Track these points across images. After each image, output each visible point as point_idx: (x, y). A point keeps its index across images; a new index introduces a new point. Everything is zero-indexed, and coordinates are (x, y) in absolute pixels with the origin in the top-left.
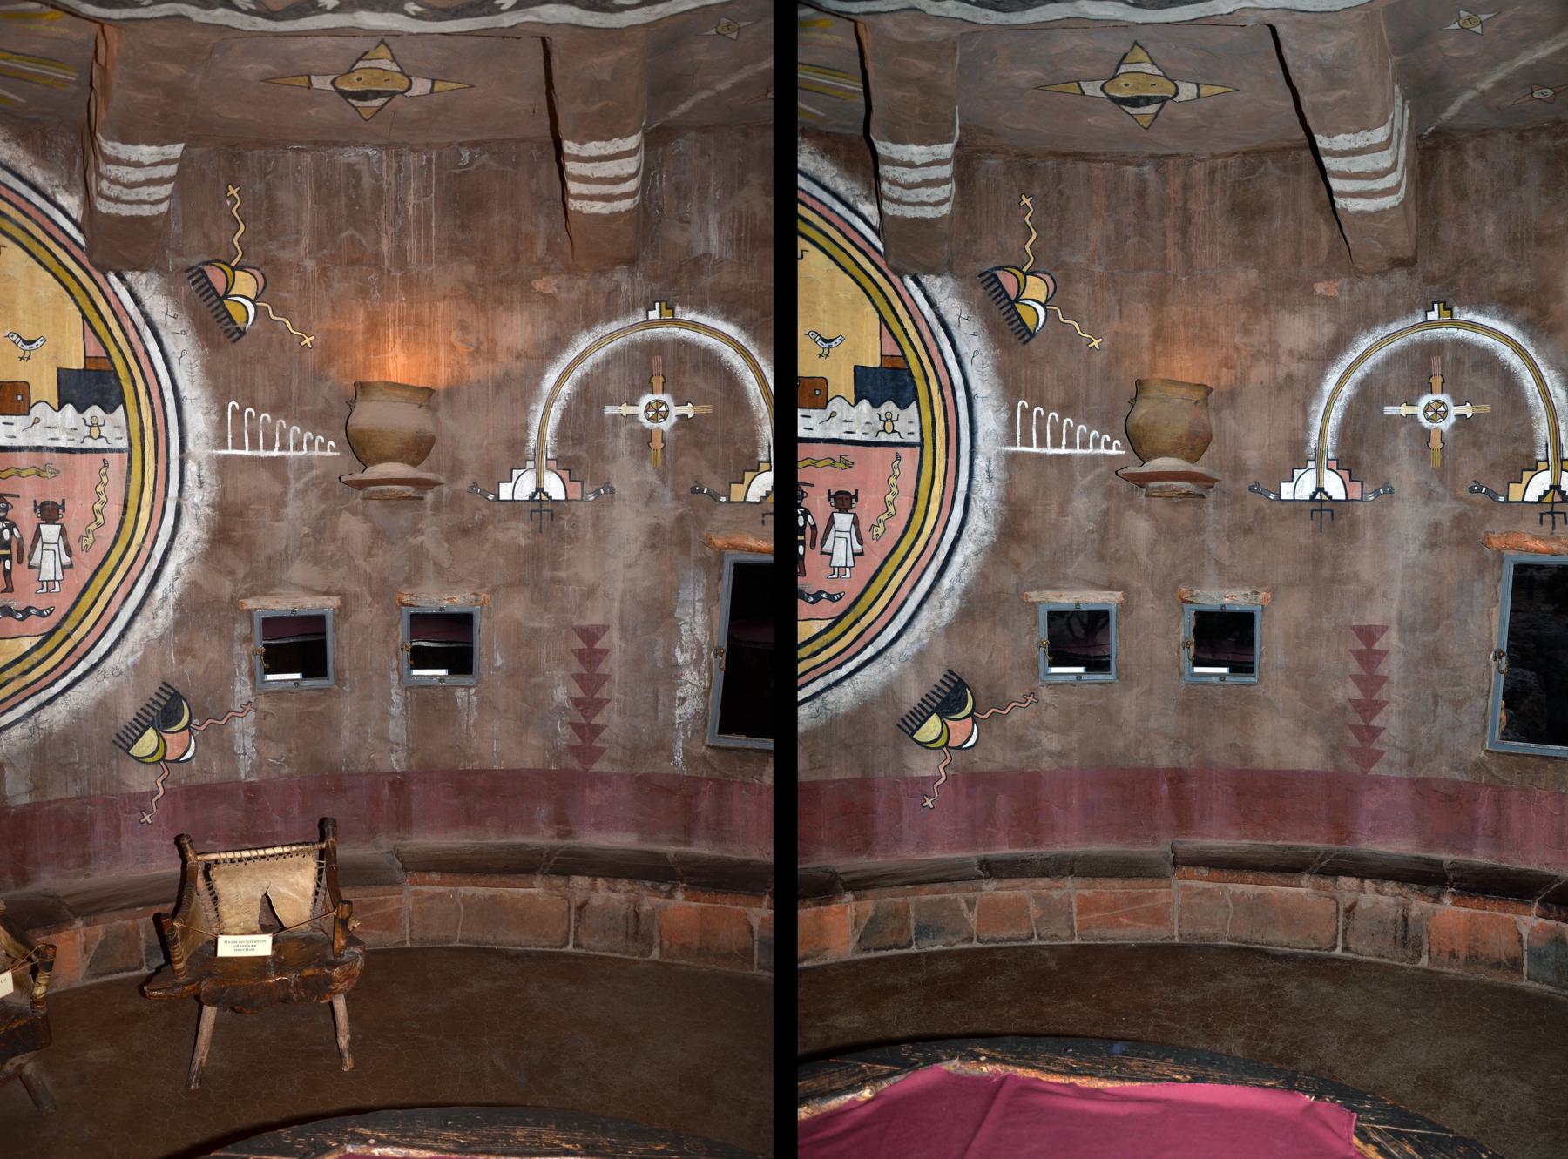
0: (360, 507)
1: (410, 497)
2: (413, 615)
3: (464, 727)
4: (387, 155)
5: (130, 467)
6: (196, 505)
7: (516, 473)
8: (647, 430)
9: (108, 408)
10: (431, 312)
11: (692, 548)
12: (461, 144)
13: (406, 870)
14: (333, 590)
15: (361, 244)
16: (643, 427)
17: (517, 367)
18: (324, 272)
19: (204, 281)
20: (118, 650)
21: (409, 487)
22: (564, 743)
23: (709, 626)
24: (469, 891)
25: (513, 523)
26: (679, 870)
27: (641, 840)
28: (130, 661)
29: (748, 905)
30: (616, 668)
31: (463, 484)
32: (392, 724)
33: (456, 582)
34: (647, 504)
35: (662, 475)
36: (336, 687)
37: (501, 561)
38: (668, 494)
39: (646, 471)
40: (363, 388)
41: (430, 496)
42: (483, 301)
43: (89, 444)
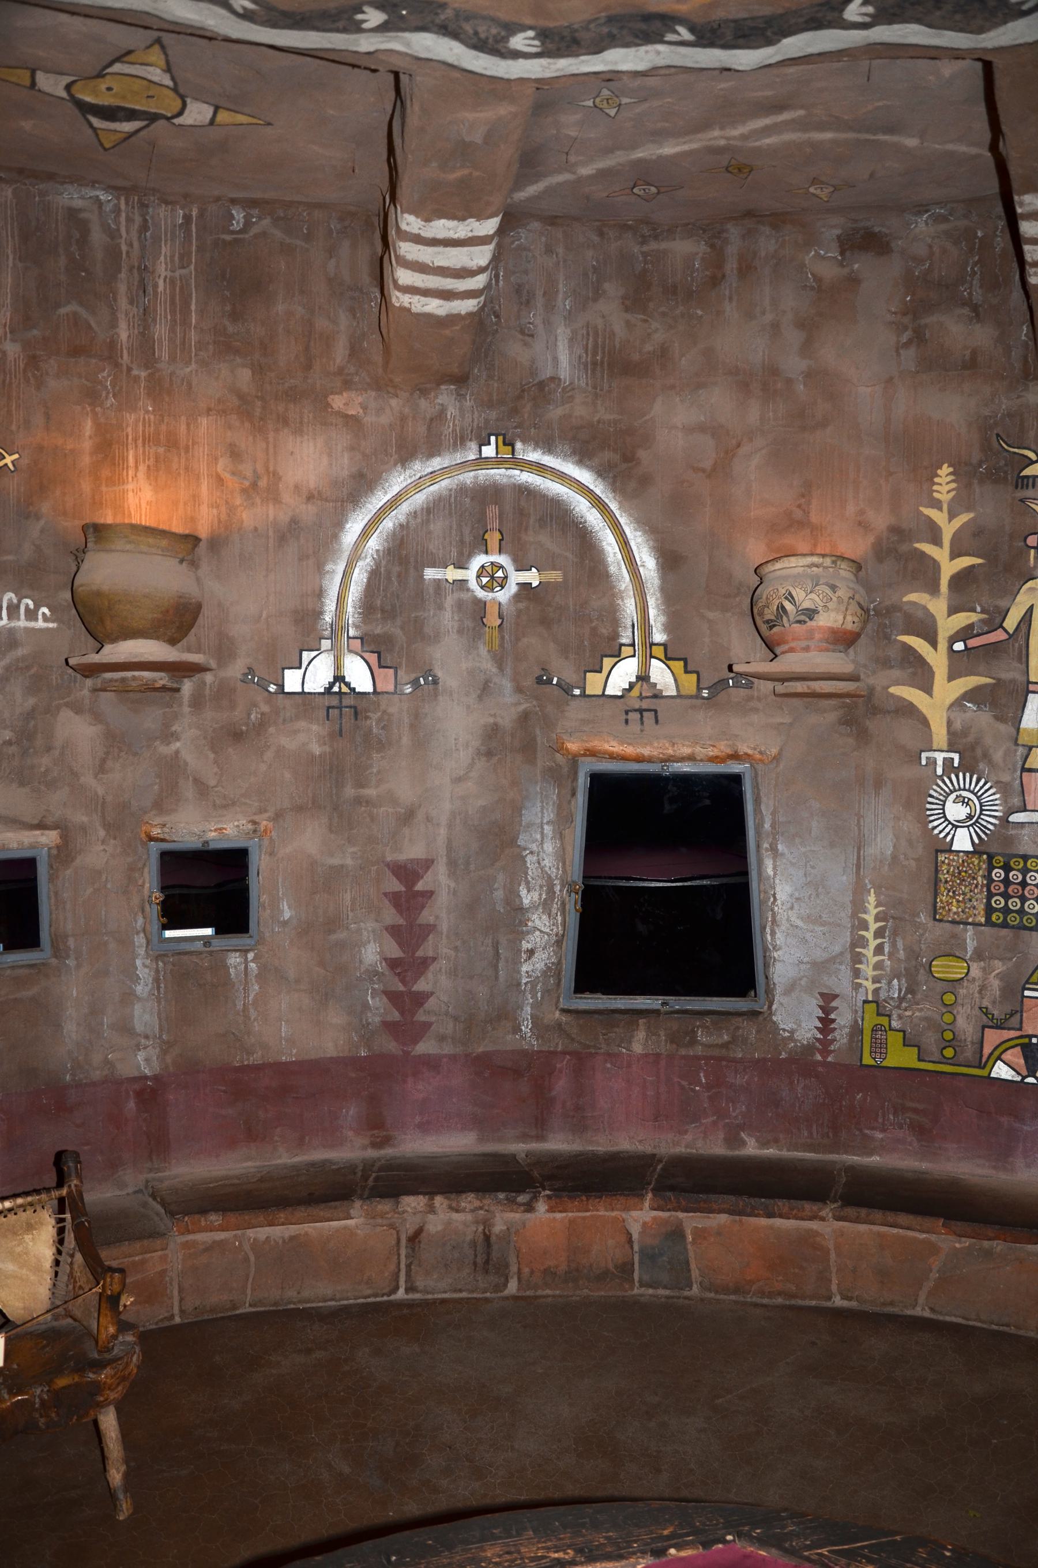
0: (87, 701)
1: (164, 689)
2: (165, 855)
3: (240, 1006)
4: (127, 203)
7: (306, 656)
10: (188, 429)
11: (539, 755)
12: (233, 201)
13: (172, 1214)
14: (50, 820)
15: (90, 327)
16: (475, 597)
17: (308, 512)
18: (33, 361)
21: (163, 674)
22: (377, 1019)
23: (561, 856)
24: (262, 1233)
25: (302, 724)
26: (536, 1174)
27: (481, 1140)
29: (627, 1209)
30: (444, 915)
31: (236, 670)
32: (138, 1009)
33: (225, 807)
34: (480, 698)
35: (499, 661)
36: (54, 961)
37: (288, 775)
38: (507, 685)
39: (479, 655)
40: (97, 532)
41: (187, 687)
42: (261, 419)
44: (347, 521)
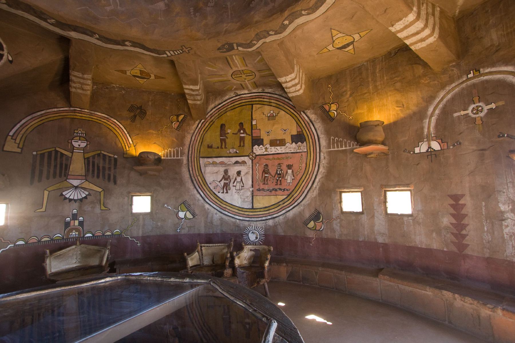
5: (307, 156)
6: (323, 164)
7: (420, 144)
8: (473, 118)
9: (302, 143)
16: (472, 117)
19: (323, 109)
20: (304, 200)
28: (307, 202)
43: (298, 151)
44: (428, 109)
